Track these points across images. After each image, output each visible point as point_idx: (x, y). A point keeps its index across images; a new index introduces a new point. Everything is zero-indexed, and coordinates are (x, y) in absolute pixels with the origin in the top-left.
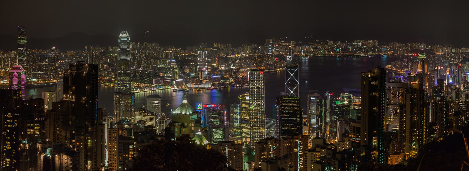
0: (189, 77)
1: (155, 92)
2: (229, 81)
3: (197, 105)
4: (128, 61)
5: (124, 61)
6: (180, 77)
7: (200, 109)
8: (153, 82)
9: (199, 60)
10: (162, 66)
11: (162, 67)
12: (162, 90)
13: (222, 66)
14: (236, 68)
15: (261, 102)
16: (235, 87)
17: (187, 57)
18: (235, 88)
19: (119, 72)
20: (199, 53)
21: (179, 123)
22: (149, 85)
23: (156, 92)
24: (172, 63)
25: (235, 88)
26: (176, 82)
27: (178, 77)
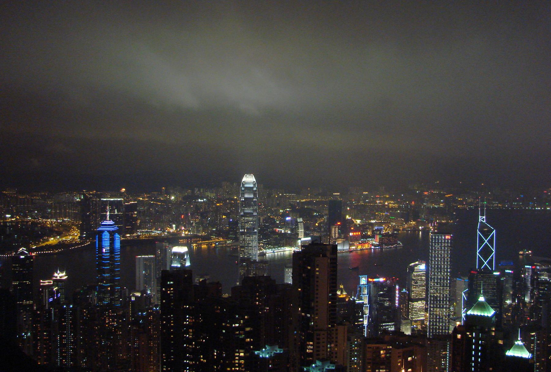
1: (273, 254)
4: (254, 216)
6: (306, 235)
7: (365, 283)
12: (282, 253)
14: (376, 222)
15: (447, 274)
17: (307, 205)
21: (478, 327)
23: (274, 254)
26: (301, 242)
27: (303, 235)
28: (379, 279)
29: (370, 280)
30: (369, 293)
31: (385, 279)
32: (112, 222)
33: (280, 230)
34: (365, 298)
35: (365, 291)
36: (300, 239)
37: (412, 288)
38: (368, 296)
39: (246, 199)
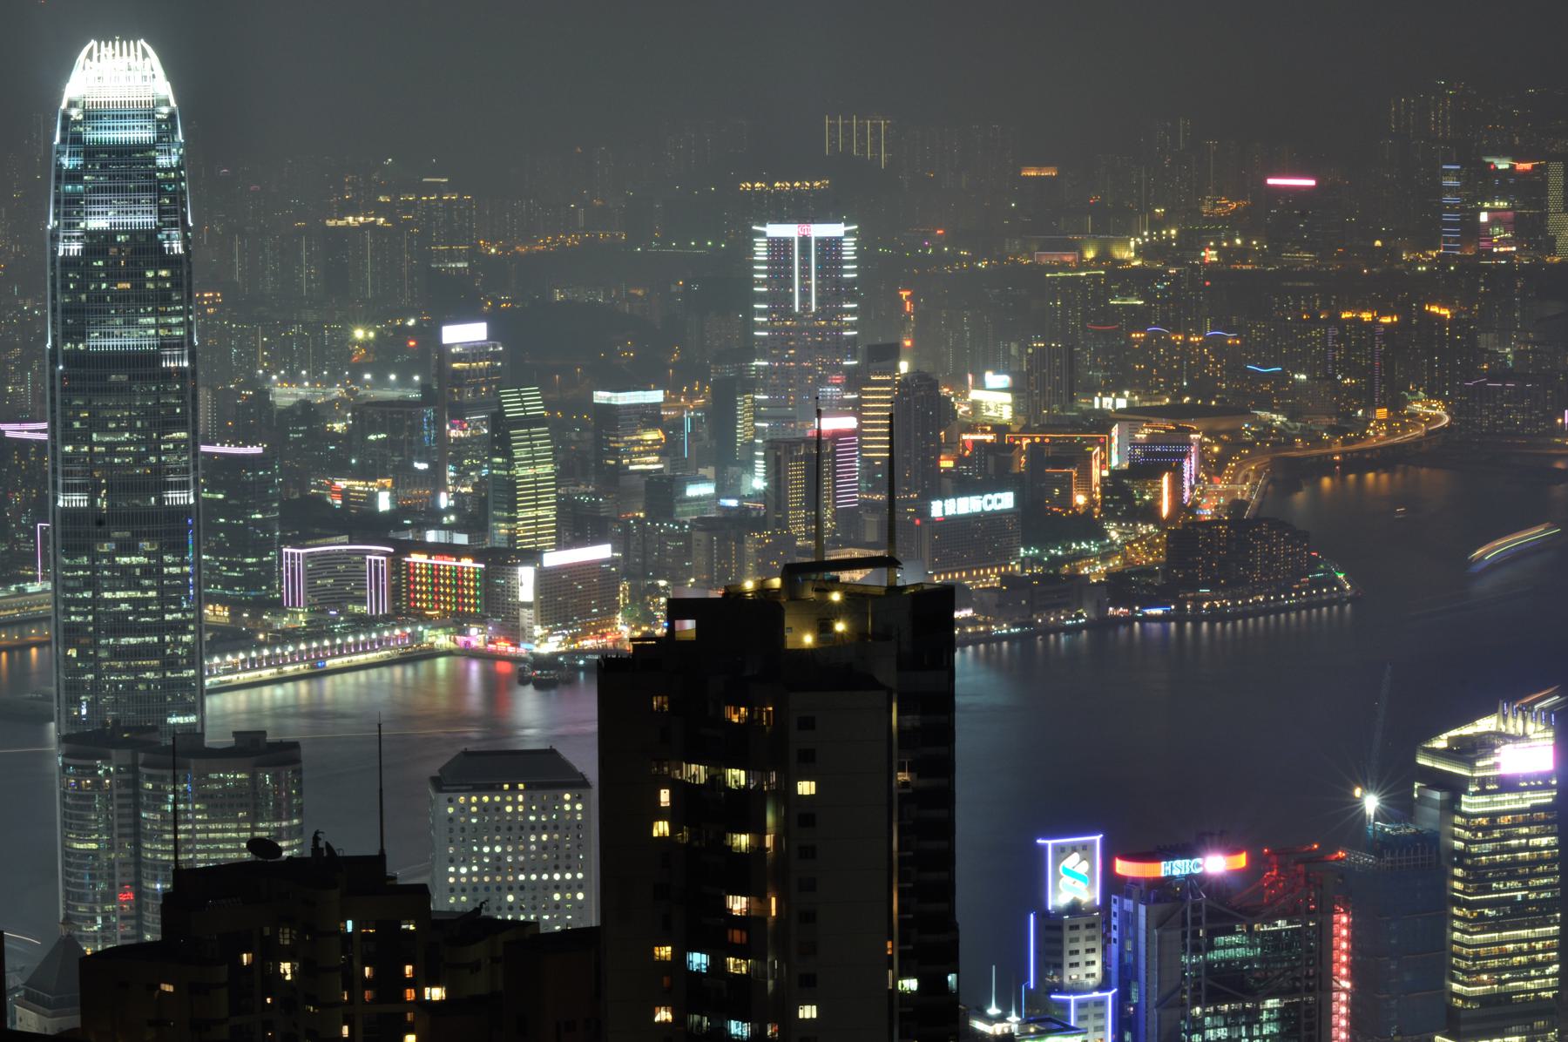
0: (669, 514)
2: (1105, 558)
3: (1057, 863)
5: (124, 378)
8: (268, 574)
9: (762, 327)
10: (302, 393)
11: (305, 405)
13: (980, 384)
16: (1180, 618)
18: (1181, 628)
19: (79, 500)
20: (761, 250)
22: (234, 615)
24: (459, 358)
25: (1181, 628)
28: (1198, 860)
29: (1122, 867)
30: (1121, 976)
31: (1241, 861)
32: (1187, 460)
33: (358, 485)
34: (1091, 1011)
35: (1091, 957)
36: (533, 556)
37: (1457, 924)
38: (1109, 995)
39: (98, 243)
